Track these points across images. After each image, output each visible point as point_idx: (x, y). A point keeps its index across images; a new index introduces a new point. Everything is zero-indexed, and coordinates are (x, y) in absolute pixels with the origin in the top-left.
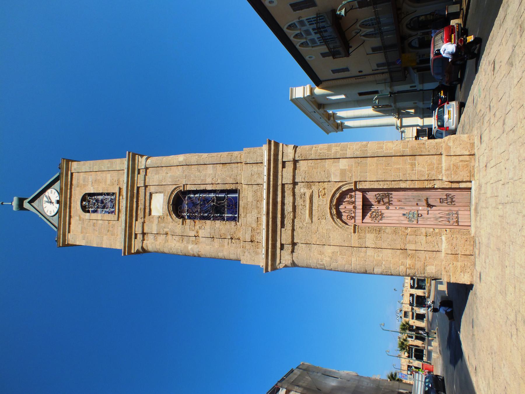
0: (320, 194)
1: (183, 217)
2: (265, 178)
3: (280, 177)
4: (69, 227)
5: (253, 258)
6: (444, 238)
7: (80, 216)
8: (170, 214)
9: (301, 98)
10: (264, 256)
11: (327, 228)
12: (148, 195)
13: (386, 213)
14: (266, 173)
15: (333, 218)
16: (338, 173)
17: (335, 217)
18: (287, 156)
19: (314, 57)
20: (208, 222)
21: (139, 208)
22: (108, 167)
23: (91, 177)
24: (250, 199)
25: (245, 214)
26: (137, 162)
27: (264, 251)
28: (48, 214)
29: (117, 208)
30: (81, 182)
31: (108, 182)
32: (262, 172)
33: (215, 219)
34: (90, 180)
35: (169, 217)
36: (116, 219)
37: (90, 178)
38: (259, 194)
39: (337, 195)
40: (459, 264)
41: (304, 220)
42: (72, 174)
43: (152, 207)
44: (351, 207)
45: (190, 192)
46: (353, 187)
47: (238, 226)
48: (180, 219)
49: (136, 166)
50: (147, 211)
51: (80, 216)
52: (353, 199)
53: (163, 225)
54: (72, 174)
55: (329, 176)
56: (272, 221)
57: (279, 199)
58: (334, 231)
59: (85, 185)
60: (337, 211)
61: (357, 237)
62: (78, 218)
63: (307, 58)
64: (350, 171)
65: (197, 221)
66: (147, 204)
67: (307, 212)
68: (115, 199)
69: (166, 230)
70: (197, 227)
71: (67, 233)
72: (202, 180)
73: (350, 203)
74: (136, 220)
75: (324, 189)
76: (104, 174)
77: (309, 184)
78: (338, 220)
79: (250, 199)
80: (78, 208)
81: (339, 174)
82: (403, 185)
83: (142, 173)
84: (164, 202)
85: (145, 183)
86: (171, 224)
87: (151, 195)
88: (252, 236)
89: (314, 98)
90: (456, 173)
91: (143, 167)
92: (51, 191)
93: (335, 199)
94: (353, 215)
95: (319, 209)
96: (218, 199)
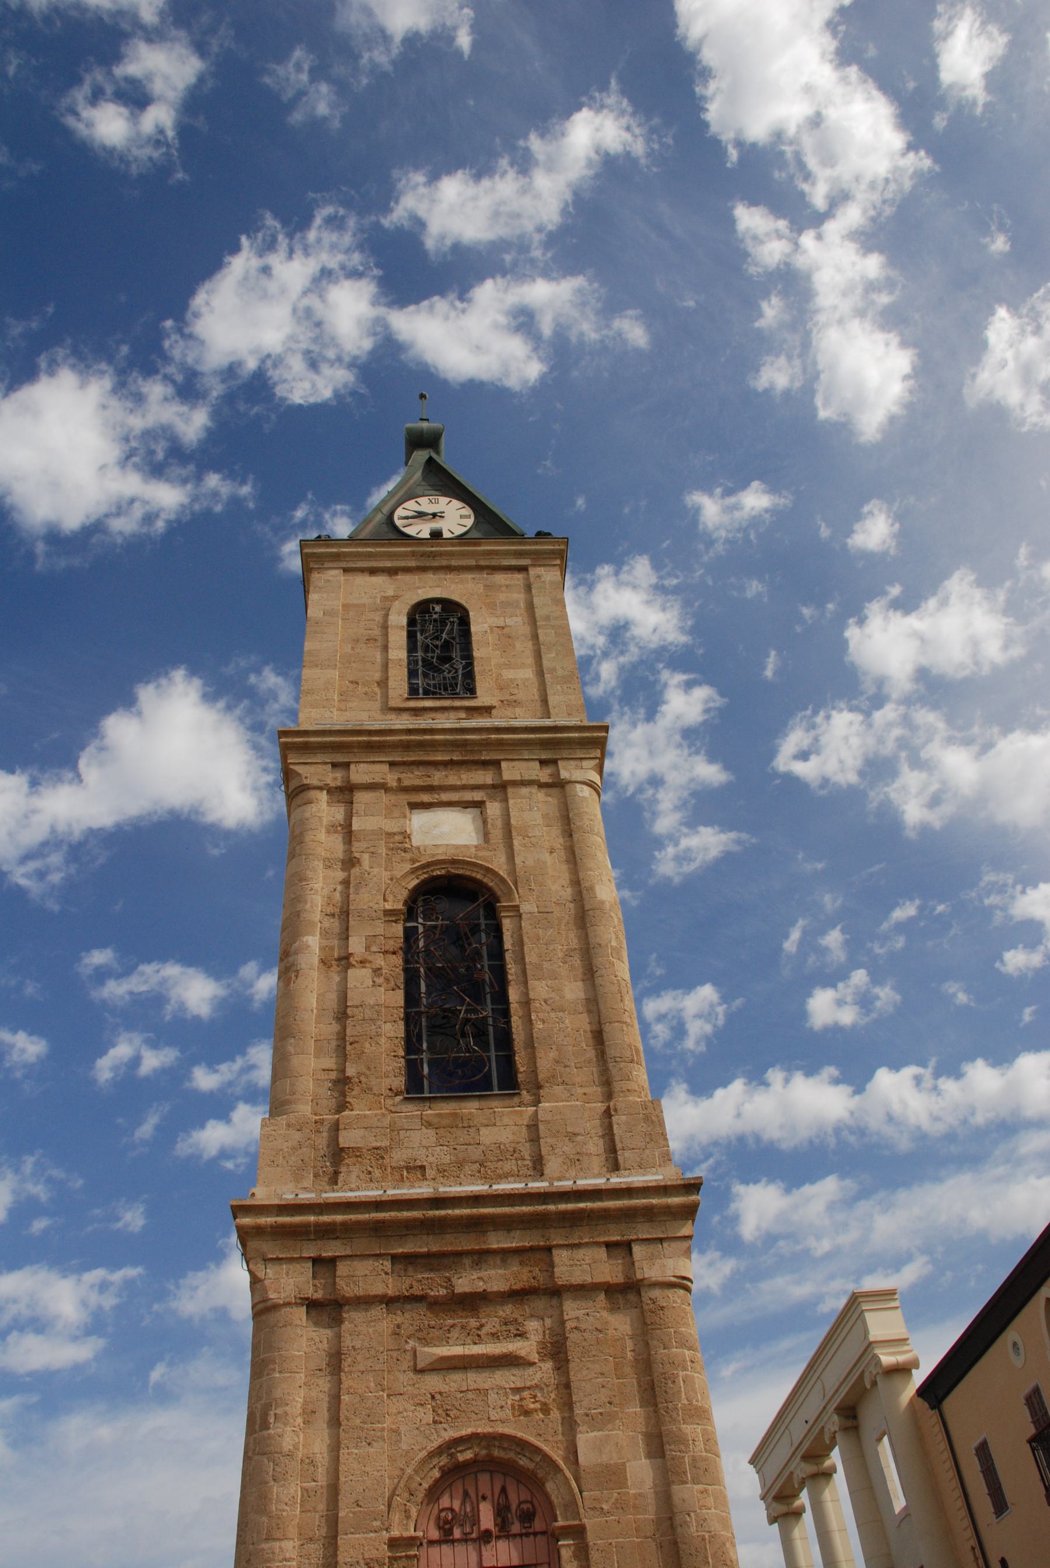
0: (526, 1394)
1: (410, 913)
2: (567, 1184)
4: (362, 570)
5: (281, 1160)
7: (396, 598)
8: (417, 869)
9: (866, 1332)
10: (289, 1197)
11: (403, 1429)
12: (478, 796)
14: (584, 1183)
15: (440, 1451)
16: (609, 1456)
17: (444, 1460)
18: (651, 1258)
19: (1018, 1362)
22: (554, 670)
23: (517, 622)
24: (488, 1136)
25: (435, 1120)
27: (306, 1197)
30: (502, 597)
31: (508, 674)
32: (586, 1173)
33: (410, 1020)
34: (509, 622)
35: (408, 867)
36: (392, 703)
37: (515, 619)
38: (509, 1166)
39: (523, 1462)
41: (425, 1341)
44: (487, 1519)
45: (497, 931)
46: (561, 1523)
47: (389, 1102)
48: (405, 903)
50: (426, 798)
51: (396, 598)
52: (516, 1528)
53: (383, 851)
54: (523, 569)
56: (415, 1220)
57: (496, 1241)
58: (392, 1459)
59: (492, 606)
60: (466, 1464)
61: (374, 1554)
62: (390, 593)
63: (1011, 1335)
64: (621, 1506)
65: (398, 960)
66: (445, 797)
67: (458, 1350)
68: (455, 696)
69: (366, 859)
70: (379, 961)
71: (344, 565)
72: (539, 967)
73: (501, 1512)
74: (392, 764)
75: (545, 1409)
76: (530, 660)
77: (557, 1350)
78: (436, 1474)
79: (488, 1136)
80: (420, 591)
81: (605, 1459)
83: (544, 775)
84: (457, 847)
85: (514, 783)
86: (385, 875)
87: (479, 805)
88: (356, 1152)
89: (874, 1383)
91: (564, 774)
92: (469, 517)
93: (511, 1455)
94: (457, 1533)
95: (470, 1395)
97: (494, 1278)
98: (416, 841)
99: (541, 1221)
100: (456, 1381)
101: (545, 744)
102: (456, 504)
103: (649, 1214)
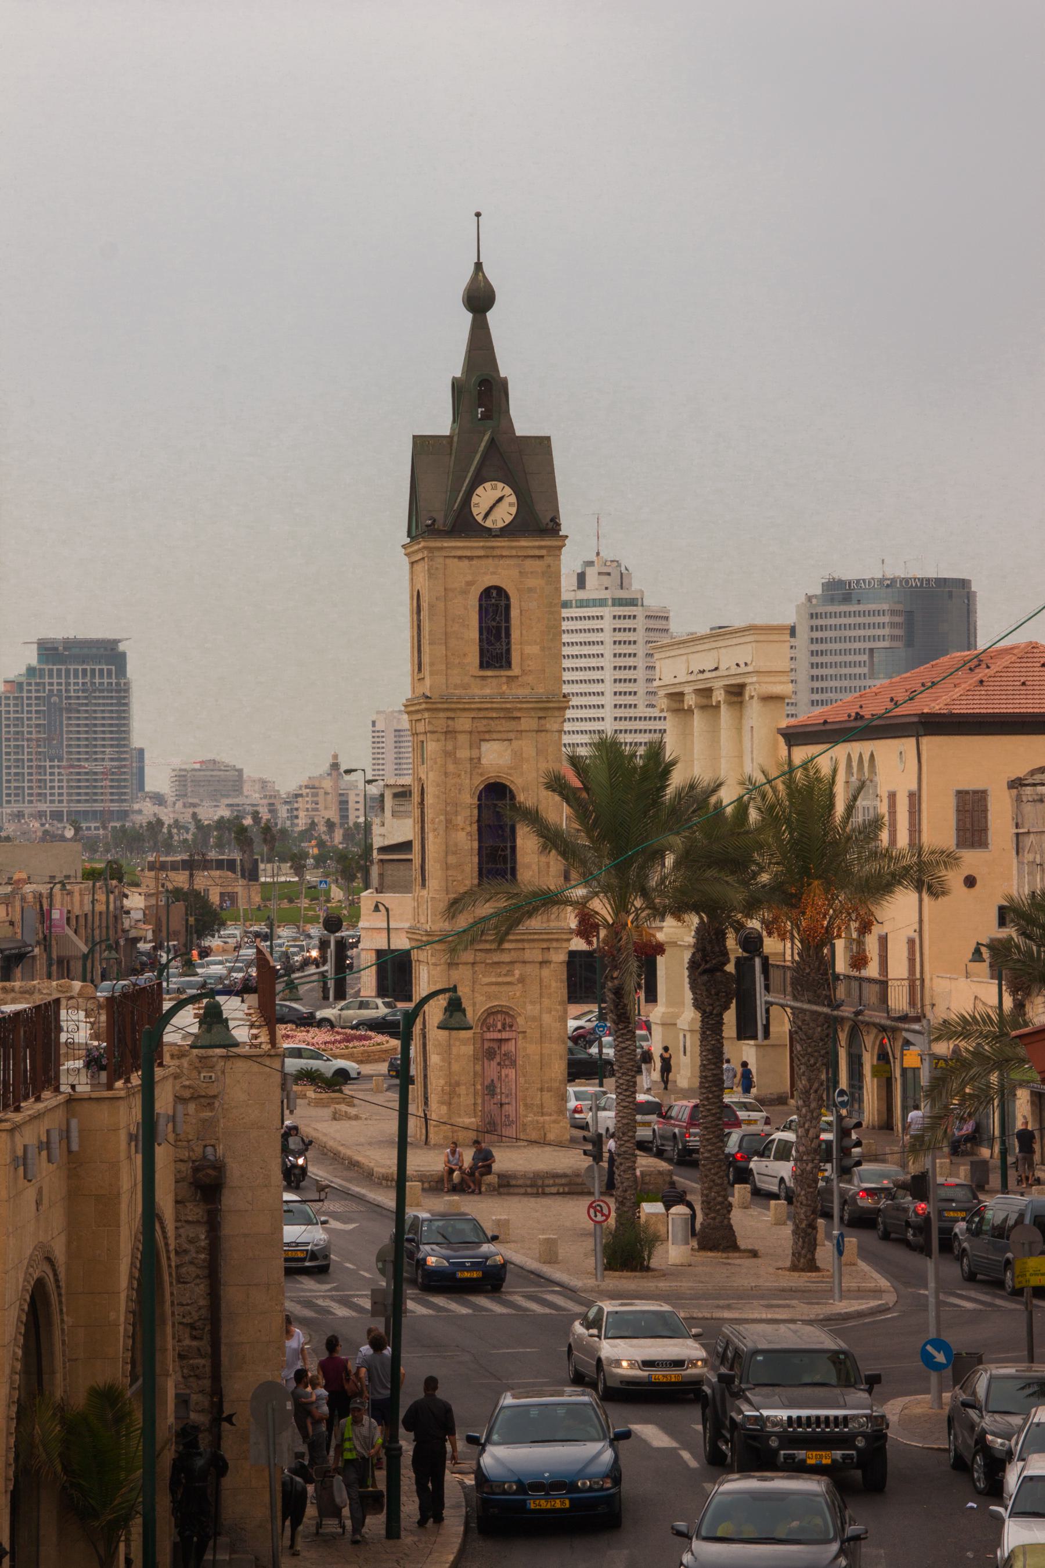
3: (532, 945)
4: (455, 557)
6: (473, 1120)
13: (494, 1064)
20: (476, 845)
21: (491, 722)
26: (557, 713)
28: (475, 499)
29: (489, 673)
40: (450, 1134)
42: (542, 557)
43: (492, 743)
44: (499, 1026)
49: (550, 713)
50: (487, 737)
55: (533, 1003)
62: (469, 578)
65: (475, 826)
67: (494, 980)
68: (501, 667)
70: (469, 829)
73: (504, 1025)
82: (522, 1080)
90: (534, 1129)
91: (548, 727)
96: (505, 857)
97: (506, 957)
98: (483, 761)
99: (523, 940)
100: (494, 989)
101: (541, 709)
102: (508, 490)
103: (557, 940)
